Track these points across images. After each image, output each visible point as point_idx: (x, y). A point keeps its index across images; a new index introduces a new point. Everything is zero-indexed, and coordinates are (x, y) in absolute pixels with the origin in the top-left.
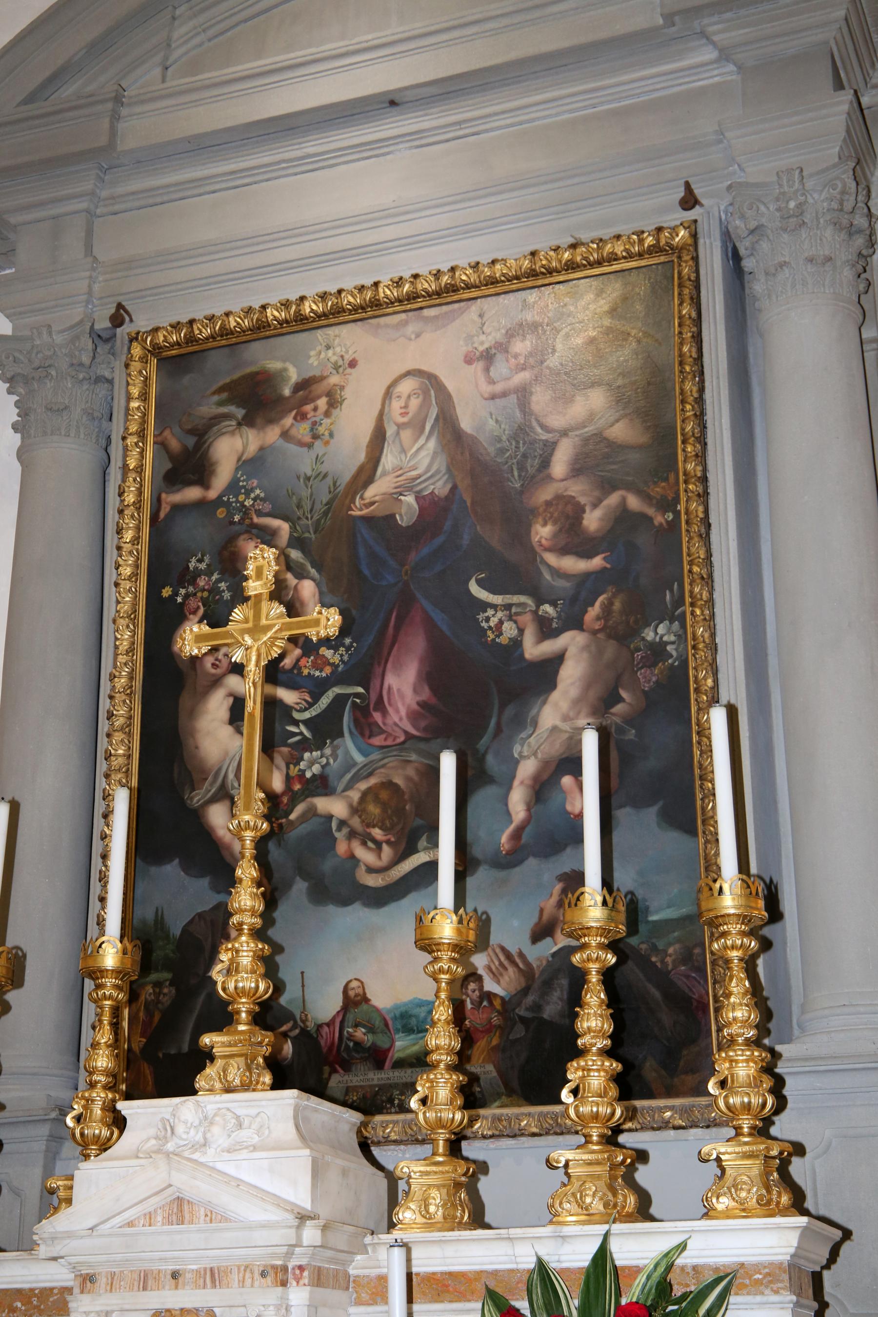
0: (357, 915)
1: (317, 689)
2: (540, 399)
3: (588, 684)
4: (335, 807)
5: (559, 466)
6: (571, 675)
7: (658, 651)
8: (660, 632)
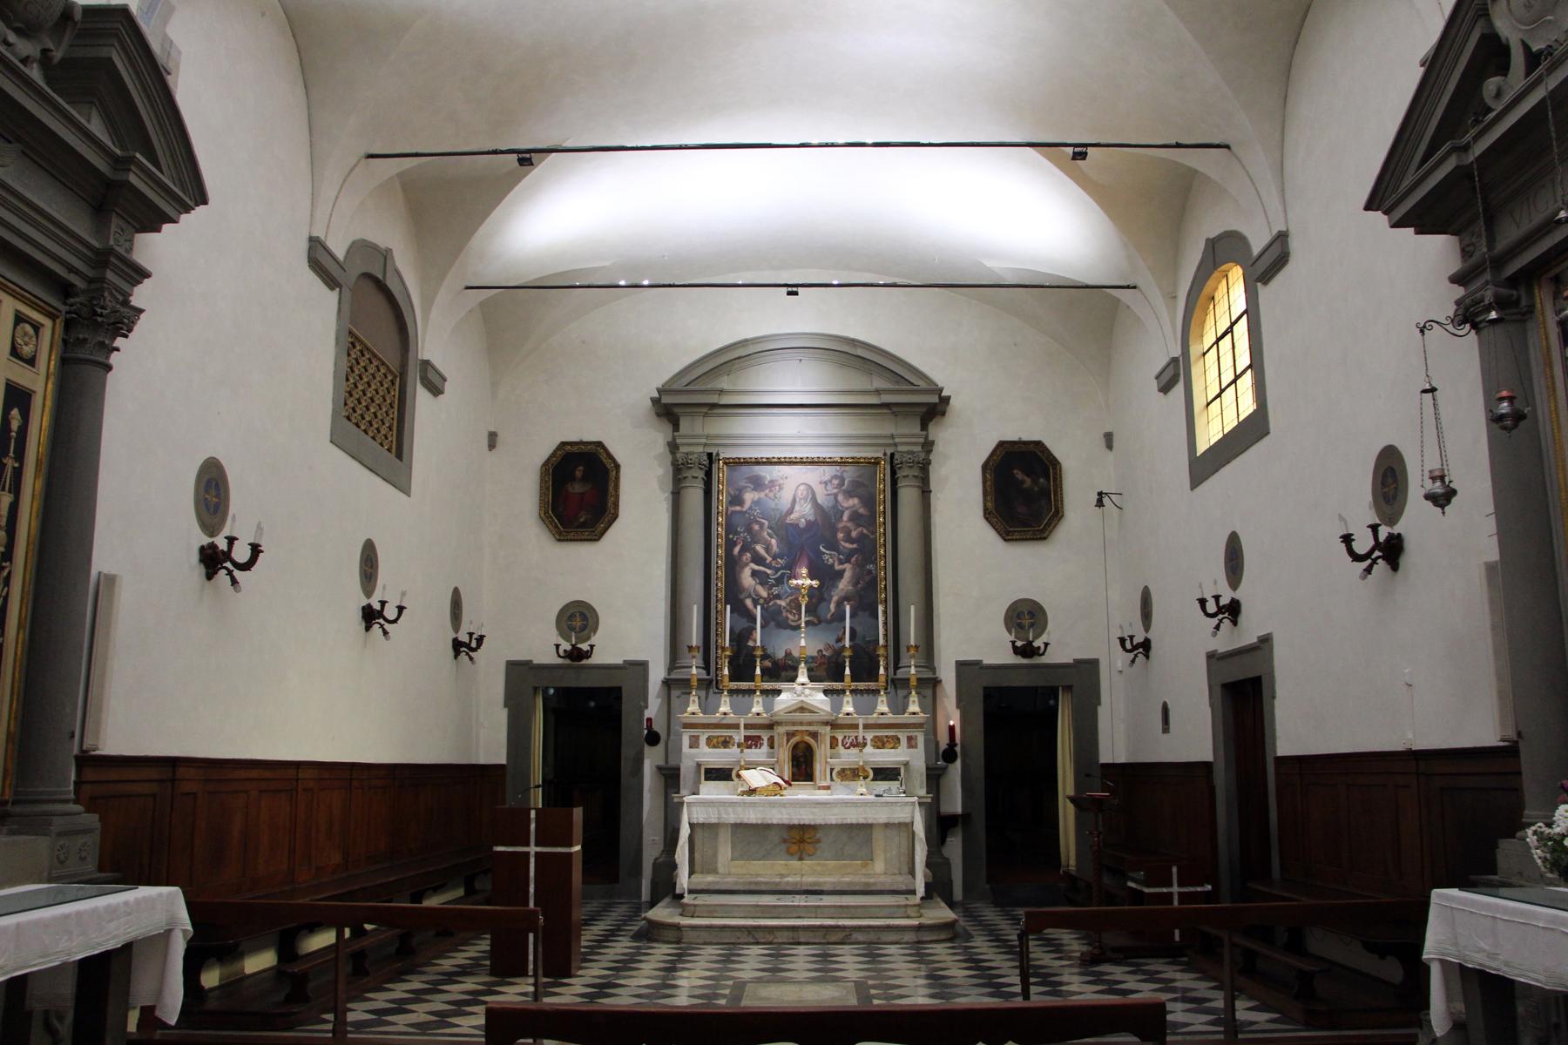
0: (788, 632)
1: (777, 570)
2: (840, 498)
3: (853, 576)
4: (783, 603)
5: (845, 518)
6: (847, 575)
7: (870, 572)
8: (871, 567)
